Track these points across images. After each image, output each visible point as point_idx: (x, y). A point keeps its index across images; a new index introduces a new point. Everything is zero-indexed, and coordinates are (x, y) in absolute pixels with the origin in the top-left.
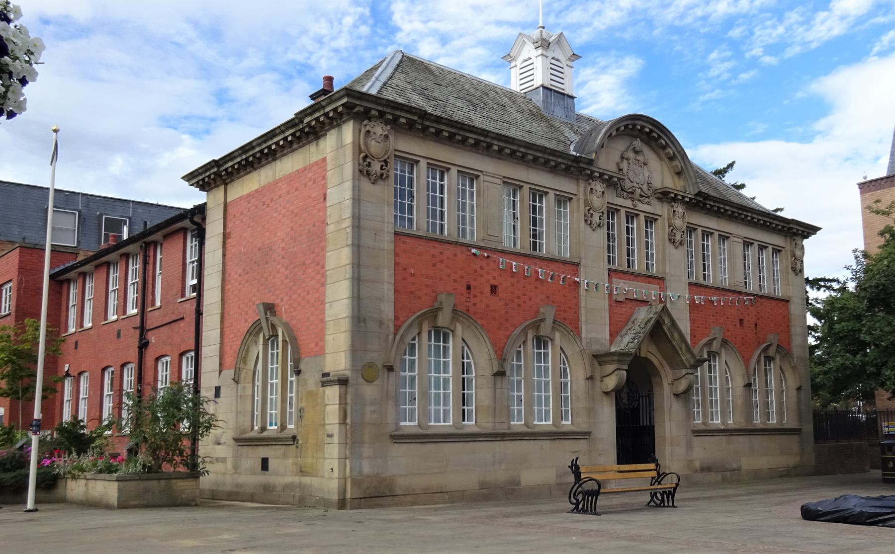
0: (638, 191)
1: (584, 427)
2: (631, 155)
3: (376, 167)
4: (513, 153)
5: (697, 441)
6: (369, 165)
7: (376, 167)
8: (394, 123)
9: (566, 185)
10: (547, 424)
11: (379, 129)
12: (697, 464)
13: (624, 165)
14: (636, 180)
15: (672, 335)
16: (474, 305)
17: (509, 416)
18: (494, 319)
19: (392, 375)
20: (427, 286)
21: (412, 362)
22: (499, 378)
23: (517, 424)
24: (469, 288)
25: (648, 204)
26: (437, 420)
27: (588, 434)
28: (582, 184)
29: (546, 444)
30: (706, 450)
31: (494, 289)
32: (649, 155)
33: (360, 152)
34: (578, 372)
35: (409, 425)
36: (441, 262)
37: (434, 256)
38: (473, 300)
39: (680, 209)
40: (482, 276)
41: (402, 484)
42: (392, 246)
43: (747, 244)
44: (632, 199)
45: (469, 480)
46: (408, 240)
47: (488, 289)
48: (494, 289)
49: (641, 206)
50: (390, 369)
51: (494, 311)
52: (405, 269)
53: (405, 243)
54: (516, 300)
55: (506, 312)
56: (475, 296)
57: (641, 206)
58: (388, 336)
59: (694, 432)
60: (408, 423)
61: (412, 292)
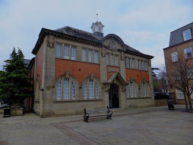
0: (113, 50)
1: (101, 99)
2: (112, 42)
3: (51, 45)
4: (89, 43)
5: (127, 100)
7: (51, 45)
8: (55, 36)
9: (97, 48)
11: (52, 37)
12: (128, 106)
13: (110, 44)
15: (121, 78)
17: (83, 96)
19: (54, 89)
20: (63, 69)
21: (60, 86)
22: (80, 89)
23: (85, 98)
24: (74, 70)
26: (66, 98)
27: (102, 100)
28: (100, 48)
29: (92, 102)
30: (129, 102)
31: (80, 70)
32: (115, 42)
33: (48, 41)
34: (100, 88)
35: (59, 99)
36: (67, 64)
37: (65, 63)
39: (123, 53)
41: (56, 112)
42: (55, 61)
43: (139, 60)
45: (73, 111)
46: (59, 60)
47: (78, 70)
48: (80, 70)
49: (114, 53)
50: (54, 87)
56: (75, 71)
57: (114, 53)
59: (127, 99)
61: (60, 71)
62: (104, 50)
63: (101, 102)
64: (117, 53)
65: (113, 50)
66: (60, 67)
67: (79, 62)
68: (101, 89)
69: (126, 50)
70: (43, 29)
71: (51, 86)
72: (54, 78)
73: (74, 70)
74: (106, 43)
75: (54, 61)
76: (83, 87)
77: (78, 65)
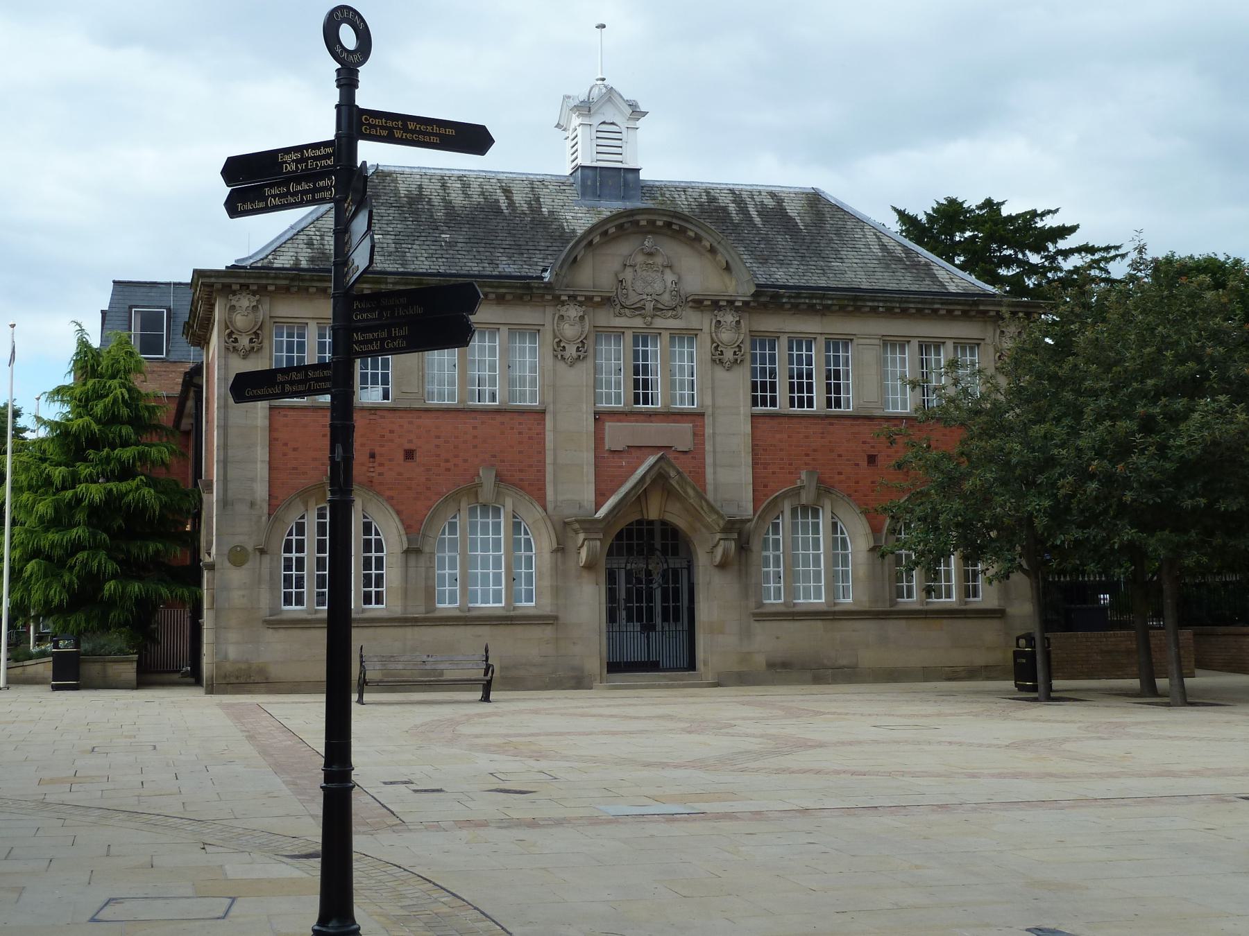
0: (649, 306)
1: (547, 610)
2: (640, 259)
5: (758, 627)
6: (236, 340)
7: (244, 341)
8: (262, 291)
9: (526, 315)
10: (819, 601)
11: (245, 302)
12: (760, 660)
13: (628, 275)
14: (649, 290)
15: (686, 492)
16: (380, 474)
17: (429, 595)
18: (409, 489)
20: (315, 459)
22: (412, 558)
23: (446, 606)
24: (373, 456)
25: (675, 317)
27: (556, 618)
28: (549, 311)
31: (409, 455)
33: (227, 327)
34: (542, 545)
38: (379, 469)
40: (392, 441)
41: (275, 672)
46: (291, 413)
47: (400, 455)
51: (409, 479)
52: (286, 444)
53: (285, 416)
54: (442, 464)
55: (428, 479)
56: (381, 465)
57: (659, 323)
58: (260, 517)
60: (447, 605)
62: (572, 323)
63: (548, 632)
64: (693, 319)
65: (649, 306)
66: (295, 449)
67: (405, 410)
68: (547, 556)
69: (756, 295)
70: (195, 271)
71: (250, 548)
72: (266, 510)
73: (378, 459)
74: (598, 273)
76: (427, 549)
77: (401, 426)
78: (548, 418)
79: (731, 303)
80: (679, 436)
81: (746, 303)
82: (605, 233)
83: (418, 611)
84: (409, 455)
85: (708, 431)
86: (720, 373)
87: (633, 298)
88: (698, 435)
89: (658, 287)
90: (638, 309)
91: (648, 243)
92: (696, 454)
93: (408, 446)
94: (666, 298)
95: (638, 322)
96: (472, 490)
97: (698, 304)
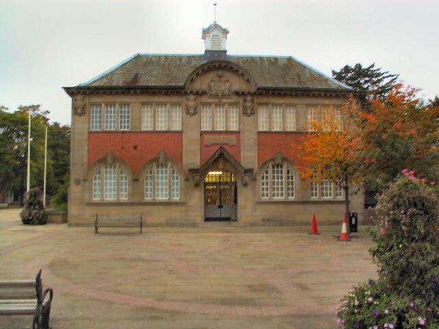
1: (184, 200)
2: (216, 79)
3: (79, 111)
7: (79, 111)
8: (84, 93)
9: (175, 99)
17: (142, 195)
19: (87, 183)
23: (148, 199)
24: (123, 148)
25: (230, 98)
29: (161, 208)
30: (262, 212)
32: (227, 75)
35: (97, 199)
39: (249, 98)
44: (218, 98)
47: (132, 147)
48: (135, 147)
50: (85, 180)
57: (224, 100)
60: (148, 198)
62: (191, 101)
64: (234, 99)
74: (200, 85)
75: (85, 136)
76: (141, 179)
78: (183, 134)
79: (249, 93)
80: (232, 140)
81: (255, 93)
82: (203, 70)
83: (137, 200)
84: (135, 147)
85: (242, 138)
86: (246, 118)
87: (214, 92)
88: (239, 140)
89: (223, 88)
90: (216, 96)
91: (220, 72)
92: (237, 147)
93: (134, 144)
94: (226, 92)
95: (216, 100)
96: (157, 160)
97: (237, 93)
